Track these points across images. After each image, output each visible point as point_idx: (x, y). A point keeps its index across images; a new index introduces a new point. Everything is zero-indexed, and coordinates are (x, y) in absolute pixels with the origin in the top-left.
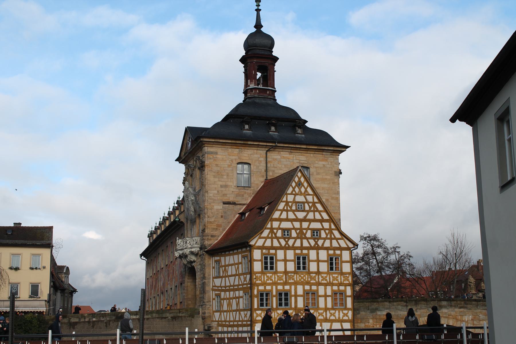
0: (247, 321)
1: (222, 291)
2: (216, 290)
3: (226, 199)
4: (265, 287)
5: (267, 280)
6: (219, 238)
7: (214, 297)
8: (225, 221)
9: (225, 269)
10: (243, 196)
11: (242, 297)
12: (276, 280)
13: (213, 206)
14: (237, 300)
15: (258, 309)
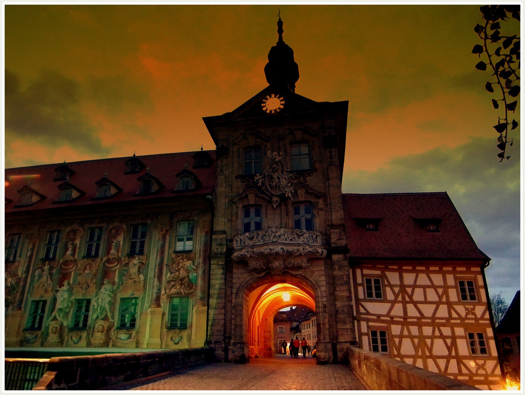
2: (367, 320)
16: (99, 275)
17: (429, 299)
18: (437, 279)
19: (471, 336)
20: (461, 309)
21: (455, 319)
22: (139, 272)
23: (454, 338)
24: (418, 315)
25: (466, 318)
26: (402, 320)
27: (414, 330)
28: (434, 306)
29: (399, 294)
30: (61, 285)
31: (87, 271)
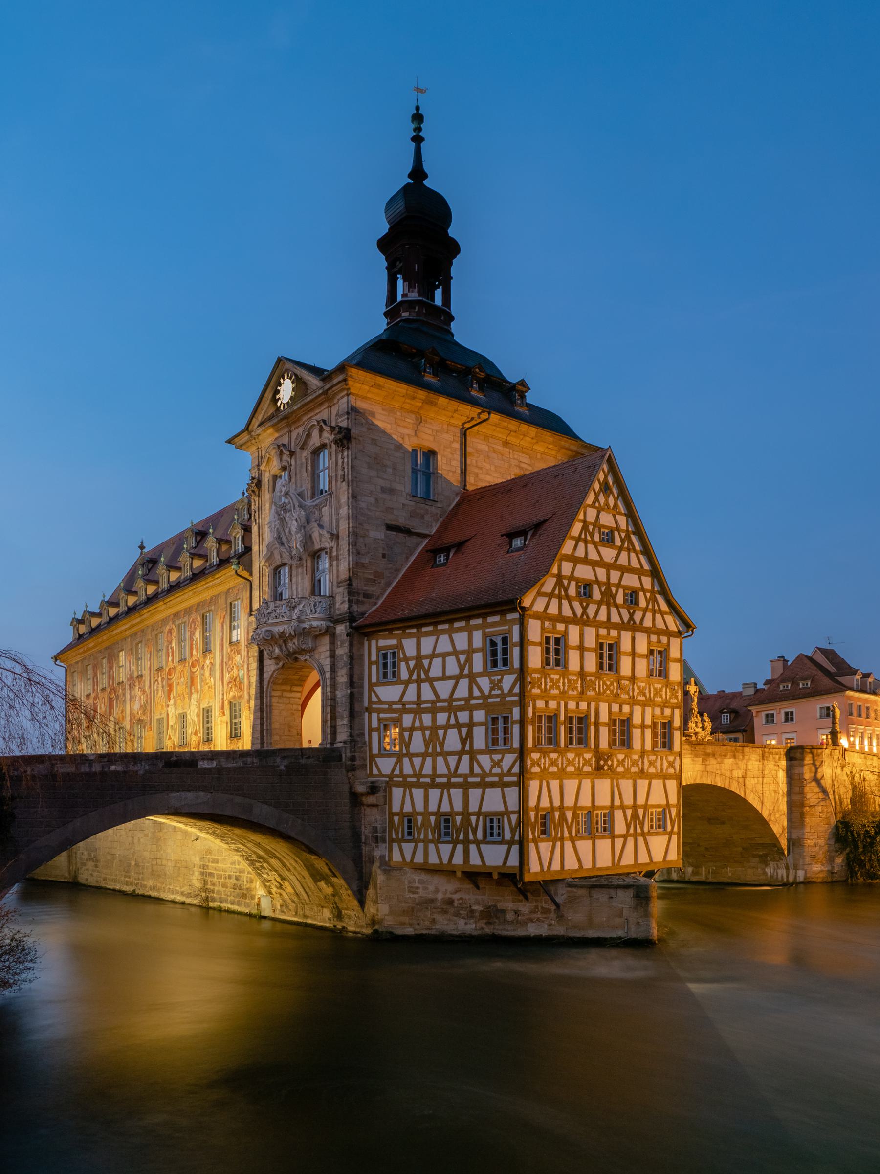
0: (501, 776)
1: (409, 711)
2: (379, 711)
3: (391, 519)
4: (547, 703)
5: (551, 687)
6: (380, 603)
7: (375, 724)
8: (390, 566)
9: (419, 666)
10: (422, 517)
11: (480, 724)
12: (566, 688)
13: (368, 530)
14: (464, 731)
15: (535, 749)
16: (189, 684)
17: (448, 673)
18: (461, 640)
19: (495, 720)
20: (484, 683)
21: (477, 698)
22: (211, 675)
23: (471, 725)
24: (433, 698)
25: (490, 696)
26: (415, 706)
27: (427, 719)
28: (453, 682)
29: (414, 669)
30: (170, 699)
31: (182, 680)
